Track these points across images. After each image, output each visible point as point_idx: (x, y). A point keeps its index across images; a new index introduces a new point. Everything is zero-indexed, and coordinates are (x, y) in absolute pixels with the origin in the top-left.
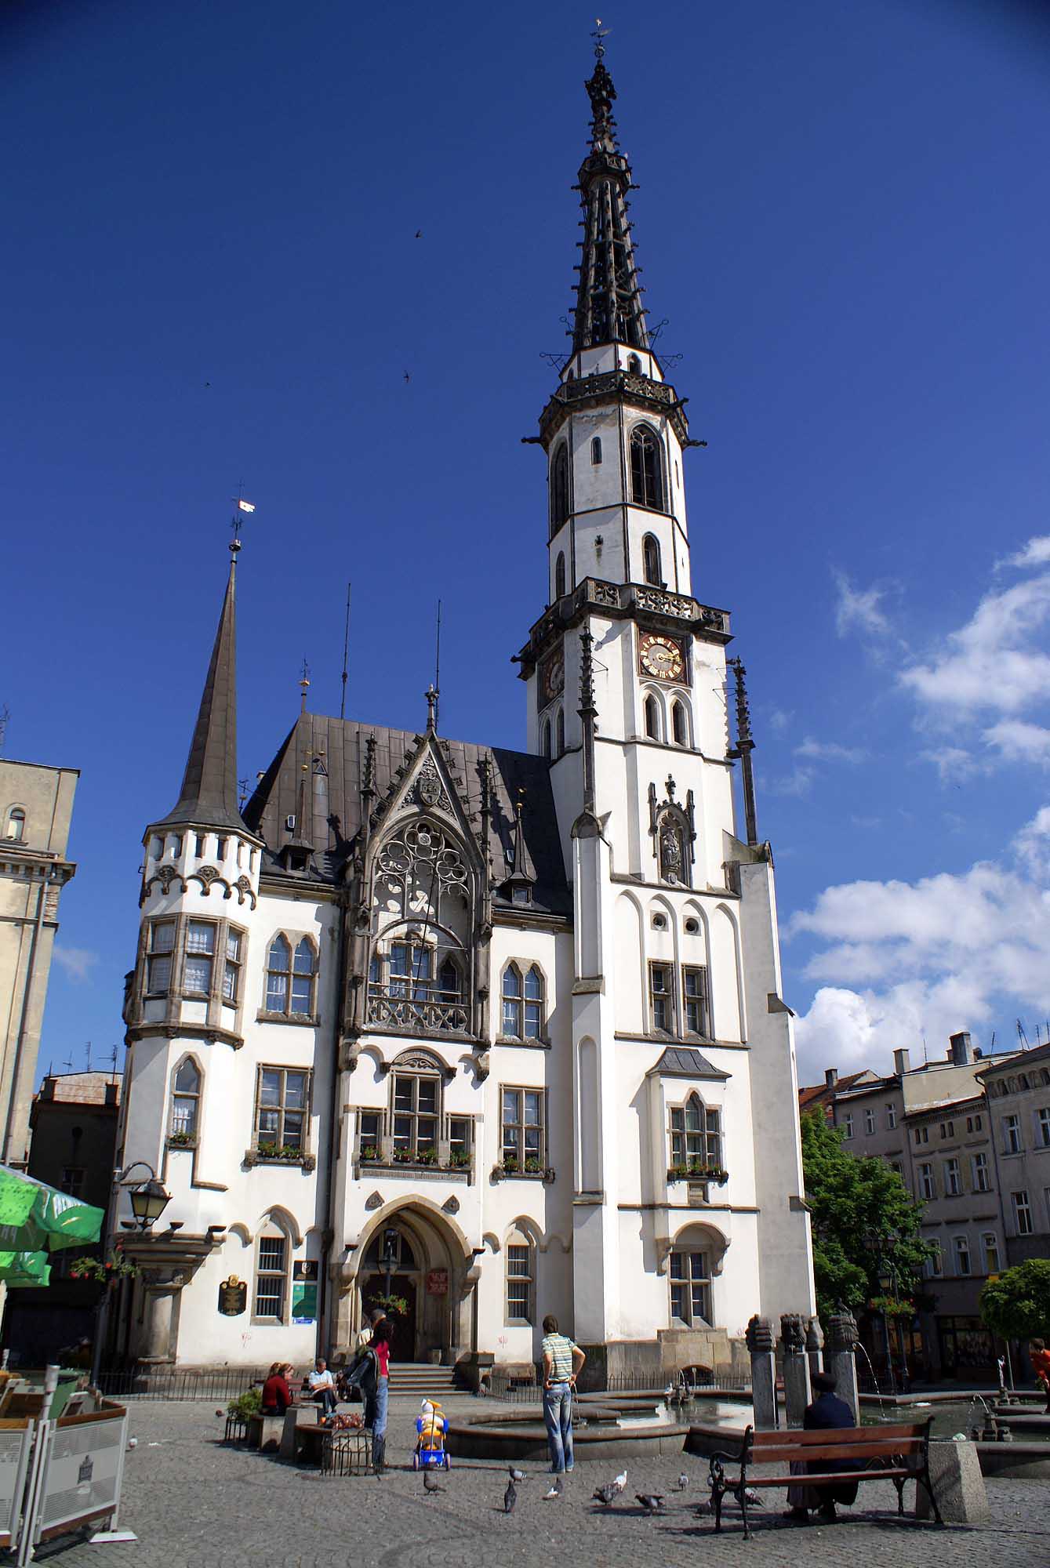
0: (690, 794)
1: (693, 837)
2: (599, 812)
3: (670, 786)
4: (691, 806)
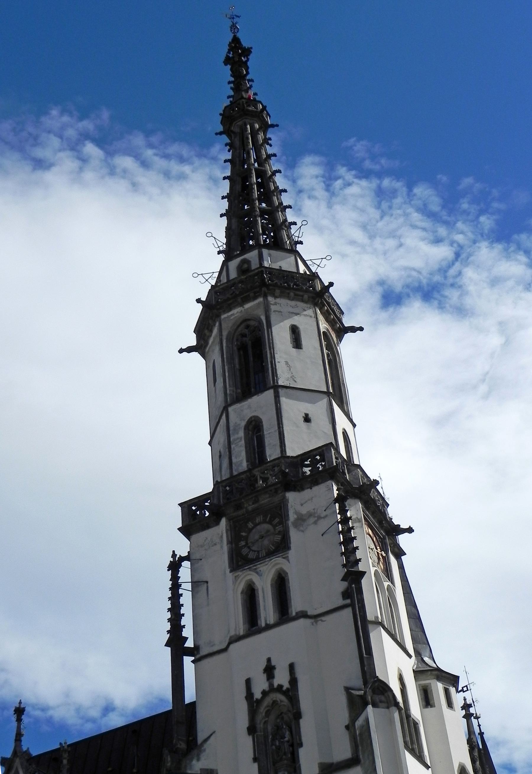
0: (292, 667)
1: (298, 715)
2: (201, 737)
3: (269, 670)
4: (294, 681)
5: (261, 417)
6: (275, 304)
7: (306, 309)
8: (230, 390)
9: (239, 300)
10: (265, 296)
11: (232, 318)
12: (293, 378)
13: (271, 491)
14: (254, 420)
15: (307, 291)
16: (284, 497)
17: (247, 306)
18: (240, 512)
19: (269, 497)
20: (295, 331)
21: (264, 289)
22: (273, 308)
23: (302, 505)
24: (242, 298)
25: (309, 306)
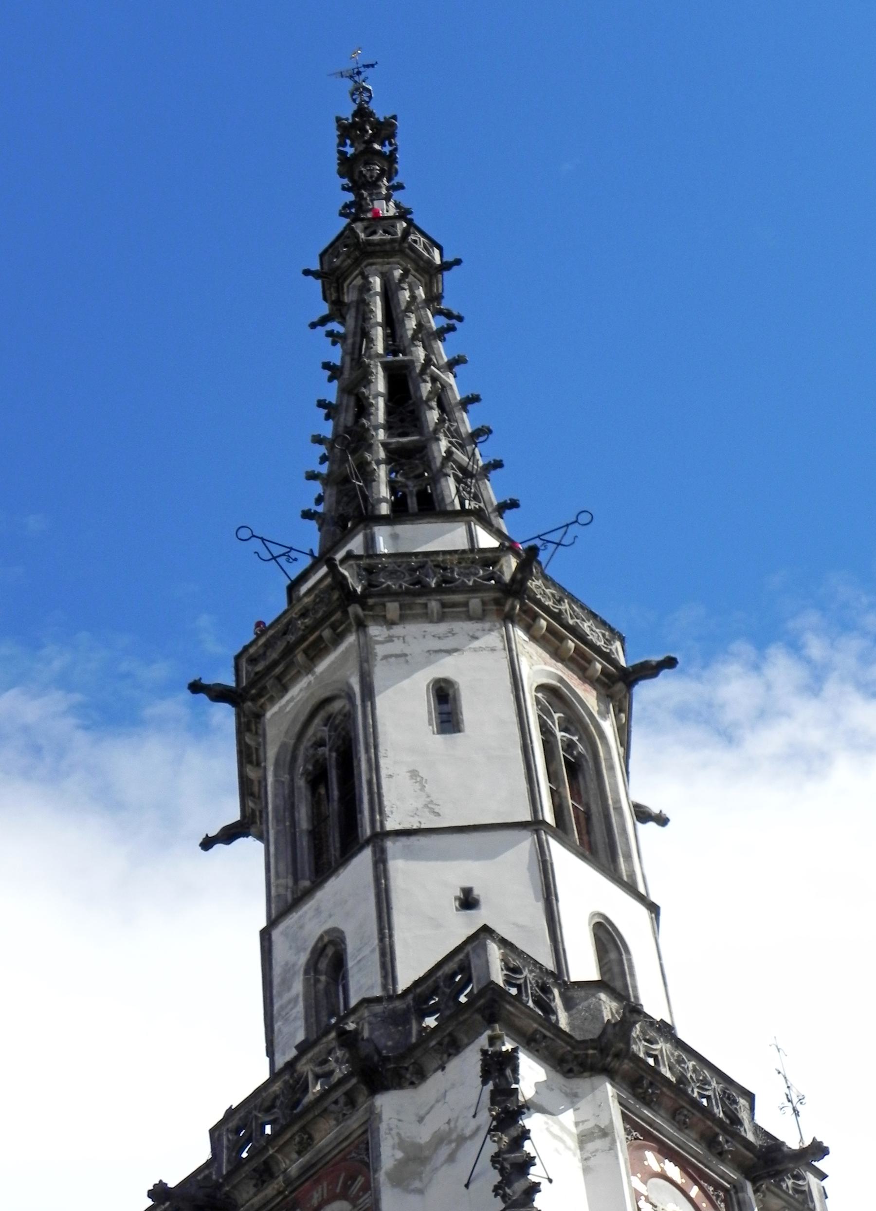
5: (342, 927)
6: (390, 639)
7: (477, 634)
8: (277, 886)
9: (300, 657)
10: (361, 625)
11: (288, 709)
12: (431, 808)
13: (336, 1102)
14: (331, 942)
15: (476, 589)
16: (371, 1110)
17: (322, 667)
18: (270, 1190)
19: (337, 1125)
20: (444, 695)
21: (355, 609)
22: (380, 650)
23: (421, 1120)
24: (305, 652)
25: (487, 625)
